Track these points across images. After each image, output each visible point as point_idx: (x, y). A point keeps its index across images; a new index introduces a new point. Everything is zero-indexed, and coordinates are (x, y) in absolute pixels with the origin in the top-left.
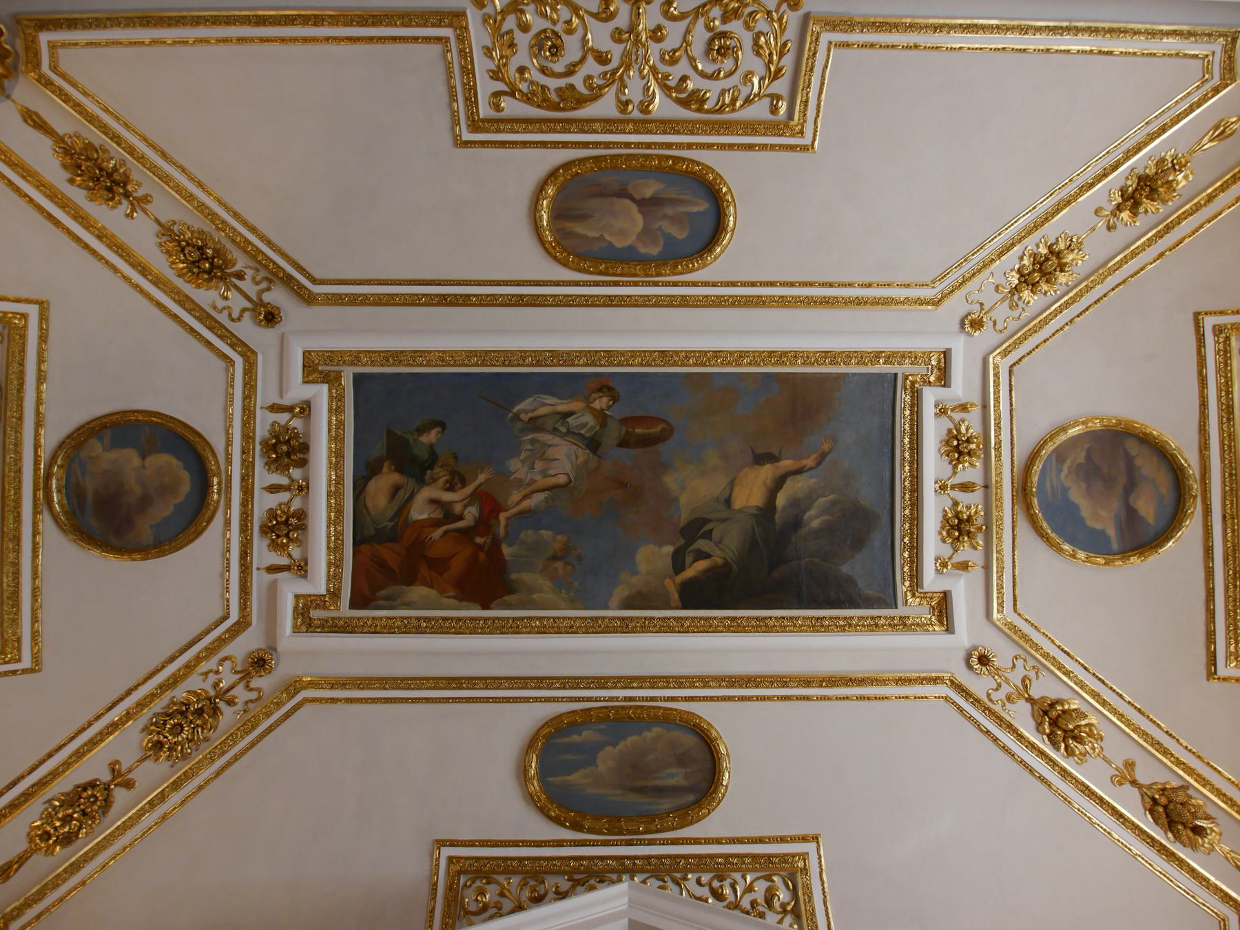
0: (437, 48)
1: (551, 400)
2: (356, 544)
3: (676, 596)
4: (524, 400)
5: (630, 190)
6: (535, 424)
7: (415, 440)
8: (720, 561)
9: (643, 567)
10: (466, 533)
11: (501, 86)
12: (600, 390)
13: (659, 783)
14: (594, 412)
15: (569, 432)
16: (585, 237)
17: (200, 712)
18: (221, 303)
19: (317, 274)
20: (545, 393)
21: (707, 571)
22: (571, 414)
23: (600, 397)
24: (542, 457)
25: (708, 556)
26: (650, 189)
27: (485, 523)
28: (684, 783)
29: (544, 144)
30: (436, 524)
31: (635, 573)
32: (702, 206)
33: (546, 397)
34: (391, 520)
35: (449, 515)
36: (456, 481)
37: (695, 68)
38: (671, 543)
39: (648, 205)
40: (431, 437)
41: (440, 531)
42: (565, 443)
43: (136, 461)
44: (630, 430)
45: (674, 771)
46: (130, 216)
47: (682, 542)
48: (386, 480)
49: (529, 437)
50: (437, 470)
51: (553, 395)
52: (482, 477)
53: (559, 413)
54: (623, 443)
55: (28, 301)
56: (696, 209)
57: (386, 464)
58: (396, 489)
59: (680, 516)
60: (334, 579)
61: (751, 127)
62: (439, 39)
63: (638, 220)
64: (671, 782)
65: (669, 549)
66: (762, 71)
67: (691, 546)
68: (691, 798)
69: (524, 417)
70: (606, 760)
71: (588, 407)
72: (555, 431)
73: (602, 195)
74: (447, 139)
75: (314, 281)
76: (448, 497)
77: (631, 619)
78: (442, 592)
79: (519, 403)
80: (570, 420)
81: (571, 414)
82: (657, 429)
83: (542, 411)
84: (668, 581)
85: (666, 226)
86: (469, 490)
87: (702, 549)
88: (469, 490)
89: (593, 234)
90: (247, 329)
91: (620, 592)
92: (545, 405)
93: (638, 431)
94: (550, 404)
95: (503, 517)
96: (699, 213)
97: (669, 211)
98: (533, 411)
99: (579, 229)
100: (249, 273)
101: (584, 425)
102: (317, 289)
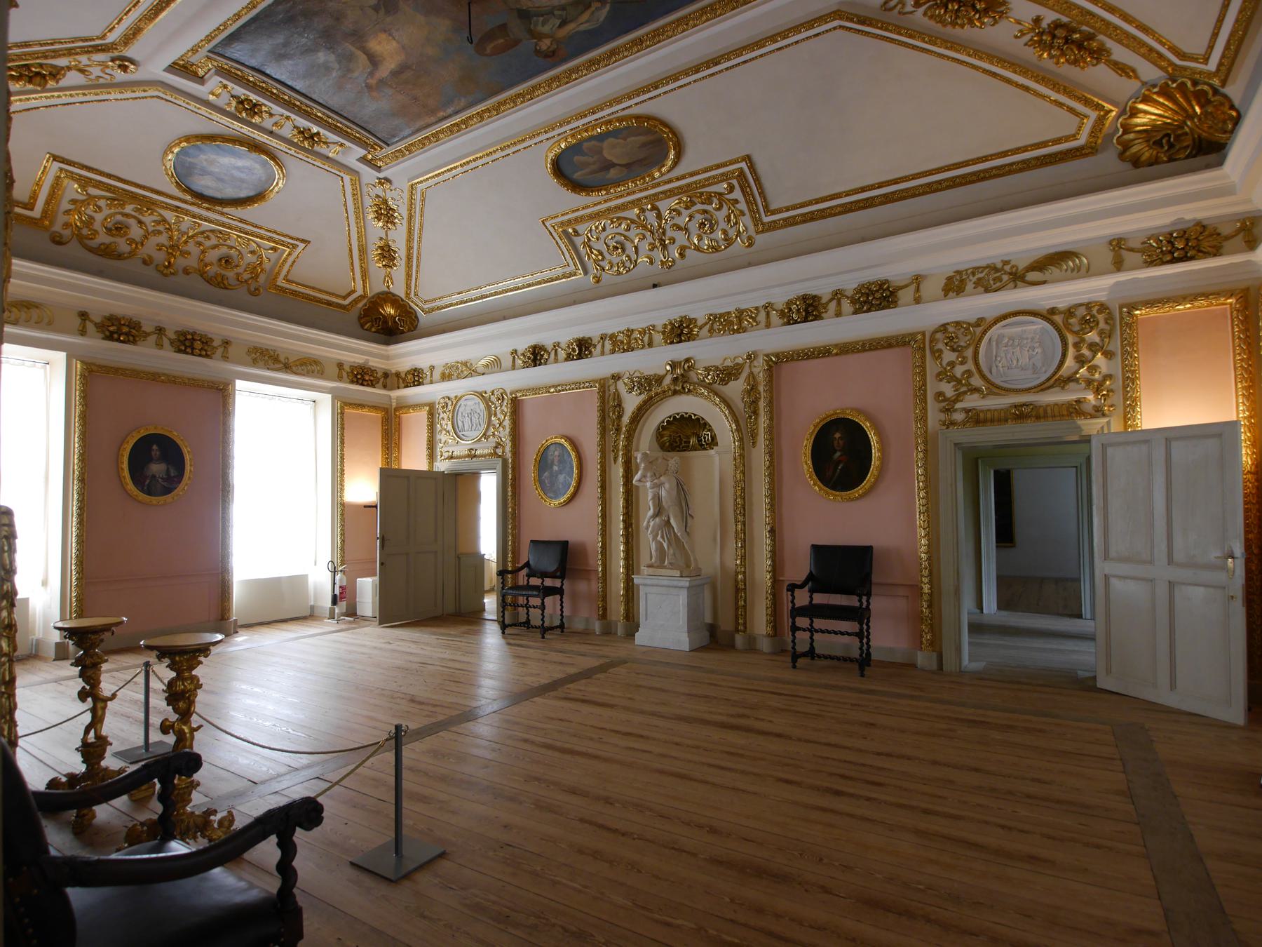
0: (773, 207)
1: (583, 27)
4: (606, 17)
5: (623, 168)
12: (554, 52)
14: (547, 36)
16: (636, 136)
19: (839, 32)
22: (561, 26)
23: (549, 47)
26: (613, 173)
29: (692, 175)
32: (577, 176)
33: (590, 28)
37: (625, 236)
39: (609, 166)
42: (548, 4)
51: (585, 32)
53: (571, 21)
54: (503, 27)
56: (579, 173)
62: (774, 212)
63: (608, 155)
66: (591, 243)
69: (595, 5)
71: (551, 37)
73: (640, 161)
74: (757, 159)
75: (842, 27)
79: (609, 12)
80: (558, 22)
81: (561, 26)
82: (489, 48)
83: (586, 16)
85: (591, 160)
89: (633, 138)
92: (586, 22)
94: (584, 22)
96: (577, 172)
97: (594, 167)
98: (593, 13)
99: (642, 139)
101: (544, 24)
102: (836, 23)
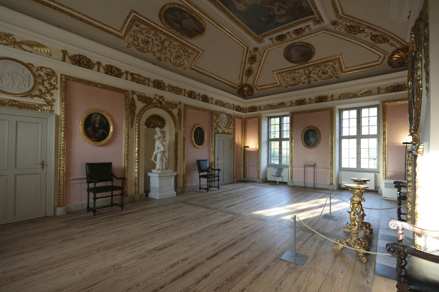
2: (297, 19)
11: (190, 55)
26: (177, 25)
30: (284, 9)
40: (263, 19)
48: (277, 20)
52: (266, 6)
58: (279, 18)
60: (308, 20)
61: (146, 24)
76: (275, 9)
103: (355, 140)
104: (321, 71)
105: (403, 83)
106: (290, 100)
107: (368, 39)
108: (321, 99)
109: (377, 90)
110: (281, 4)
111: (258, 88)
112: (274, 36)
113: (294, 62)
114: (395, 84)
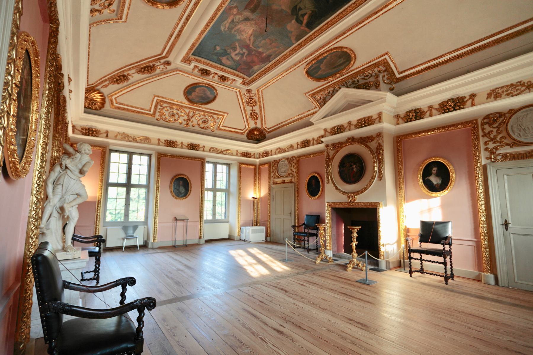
1: (225, 22)
3: (307, 29)
6: (230, 29)
7: (217, 51)
8: (310, 12)
9: (292, 30)
10: (248, 54)
13: (338, 64)
15: (238, 23)
17: (251, 101)
18: (161, 69)
19: (159, 53)
20: (223, 22)
21: (309, 17)
23: (233, 11)
24: (241, 31)
25: (305, 14)
27: (250, 51)
28: (344, 61)
31: (292, 32)
34: (235, 63)
35: (243, 54)
36: (235, 49)
38: (293, 19)
41: (245, 58)
43: (196, 93)
44: (250, 8)
45: (340, 60)
46: (133, 77)
47: (295, 17)
48: (224, 60)
49: (233, 31)
50: (228, 50)
51: (224, 21)
53: (231, 23)
55: (154, 98)
57: (220, 58)
59: (288, 12)
64: (341, 62)
65: (294, 21)
67: (298, 15)
68: (348, 63)
69: (226, 29)
70: (323, 67)
72: (236, 26)
76: (237, 52)
77: (301, 43)
78: (259, 65)
80: (235, 21)
83: (227, 25)
84: (302, 28)
86: (238, 48)
87: (302, 13)
88: (238, 48)
90: (169, 68)
91: (293, 39)
92: (226, 24)
93: (252, 7)
94: (226, 24)
95: (251, 46)
100: (154, 63)
102: (164, 55)
103: (124, 189)
104: (203, 120)
105: (250, 152)
106: (159, 138)
107: (249, 112)
108: (193, 147)
109: (157, 142)
110: (246, 54)
111: (115, 104)
112: (201, 66)
113: (189, 100)
114: (246, 152)
